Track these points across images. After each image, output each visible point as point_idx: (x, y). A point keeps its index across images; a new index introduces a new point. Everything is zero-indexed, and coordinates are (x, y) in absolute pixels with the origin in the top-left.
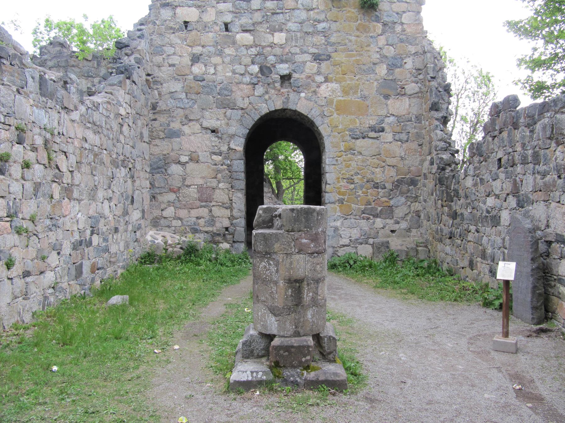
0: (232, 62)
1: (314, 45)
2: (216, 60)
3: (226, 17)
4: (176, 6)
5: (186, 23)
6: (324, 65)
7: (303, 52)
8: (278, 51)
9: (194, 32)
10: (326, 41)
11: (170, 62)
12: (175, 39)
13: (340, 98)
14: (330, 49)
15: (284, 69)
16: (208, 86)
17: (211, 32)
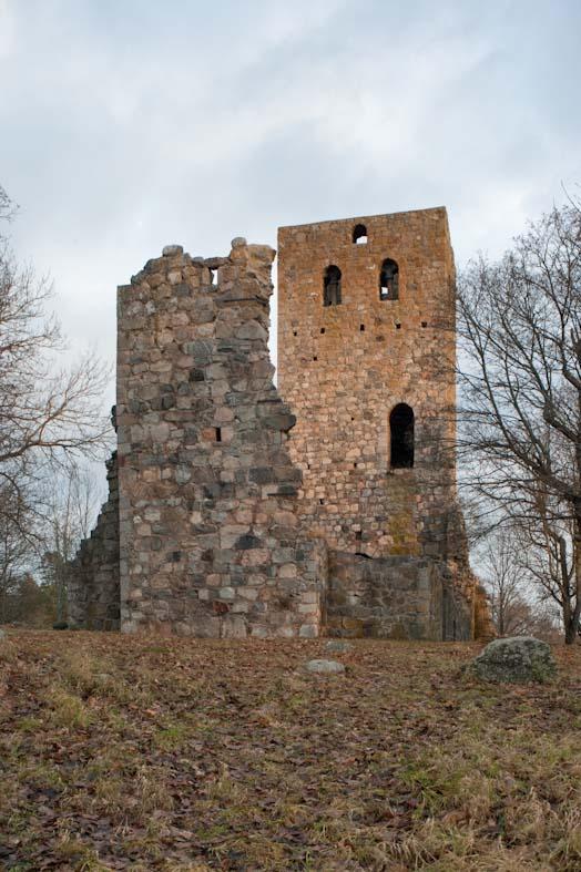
0: (324, 525)
7: (369, 516)
8: (354, 515)
15: (357, 527)
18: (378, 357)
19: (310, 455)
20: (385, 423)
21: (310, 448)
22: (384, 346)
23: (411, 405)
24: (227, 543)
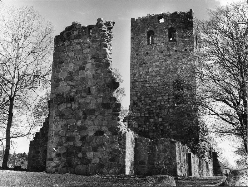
0: (148, 127)
2: (145, 126)
22: (171, 58)
24: (91, 134)
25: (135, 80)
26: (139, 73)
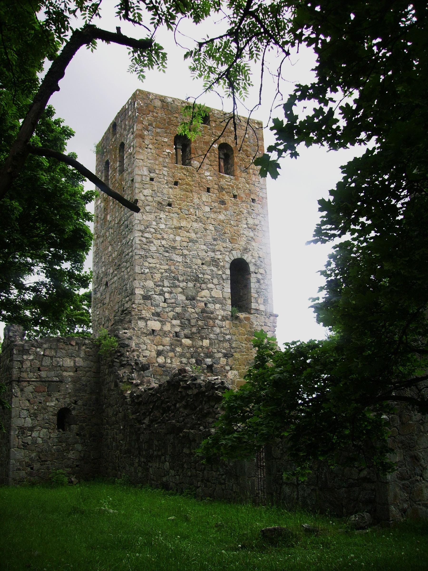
1: (224, 348)
2: (171, 354)
3: (177, 328)
4: (147, 320)
5: (153, 331)
6: (230, 360)
7: (218, 352)
9: (158, 337)
10: (230, 346)
11: (144, 355)
12: (146, 340)
13: (239, 380)
14: (232, 350)
15: (209, 361)
16: (167, 371)
17: (168, 337)
18: (222, 217)
19: (165, 289)
20: (228, 272)
21: (166, 283)
22: (226, 209)
23: (248, 261)
25: (147, 238)
26: (158, 224)
